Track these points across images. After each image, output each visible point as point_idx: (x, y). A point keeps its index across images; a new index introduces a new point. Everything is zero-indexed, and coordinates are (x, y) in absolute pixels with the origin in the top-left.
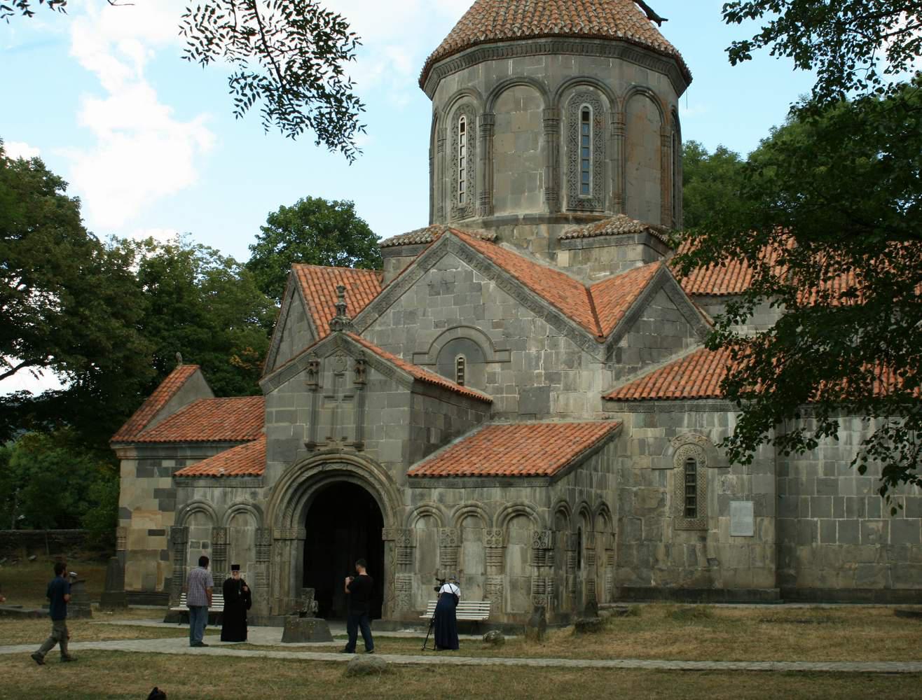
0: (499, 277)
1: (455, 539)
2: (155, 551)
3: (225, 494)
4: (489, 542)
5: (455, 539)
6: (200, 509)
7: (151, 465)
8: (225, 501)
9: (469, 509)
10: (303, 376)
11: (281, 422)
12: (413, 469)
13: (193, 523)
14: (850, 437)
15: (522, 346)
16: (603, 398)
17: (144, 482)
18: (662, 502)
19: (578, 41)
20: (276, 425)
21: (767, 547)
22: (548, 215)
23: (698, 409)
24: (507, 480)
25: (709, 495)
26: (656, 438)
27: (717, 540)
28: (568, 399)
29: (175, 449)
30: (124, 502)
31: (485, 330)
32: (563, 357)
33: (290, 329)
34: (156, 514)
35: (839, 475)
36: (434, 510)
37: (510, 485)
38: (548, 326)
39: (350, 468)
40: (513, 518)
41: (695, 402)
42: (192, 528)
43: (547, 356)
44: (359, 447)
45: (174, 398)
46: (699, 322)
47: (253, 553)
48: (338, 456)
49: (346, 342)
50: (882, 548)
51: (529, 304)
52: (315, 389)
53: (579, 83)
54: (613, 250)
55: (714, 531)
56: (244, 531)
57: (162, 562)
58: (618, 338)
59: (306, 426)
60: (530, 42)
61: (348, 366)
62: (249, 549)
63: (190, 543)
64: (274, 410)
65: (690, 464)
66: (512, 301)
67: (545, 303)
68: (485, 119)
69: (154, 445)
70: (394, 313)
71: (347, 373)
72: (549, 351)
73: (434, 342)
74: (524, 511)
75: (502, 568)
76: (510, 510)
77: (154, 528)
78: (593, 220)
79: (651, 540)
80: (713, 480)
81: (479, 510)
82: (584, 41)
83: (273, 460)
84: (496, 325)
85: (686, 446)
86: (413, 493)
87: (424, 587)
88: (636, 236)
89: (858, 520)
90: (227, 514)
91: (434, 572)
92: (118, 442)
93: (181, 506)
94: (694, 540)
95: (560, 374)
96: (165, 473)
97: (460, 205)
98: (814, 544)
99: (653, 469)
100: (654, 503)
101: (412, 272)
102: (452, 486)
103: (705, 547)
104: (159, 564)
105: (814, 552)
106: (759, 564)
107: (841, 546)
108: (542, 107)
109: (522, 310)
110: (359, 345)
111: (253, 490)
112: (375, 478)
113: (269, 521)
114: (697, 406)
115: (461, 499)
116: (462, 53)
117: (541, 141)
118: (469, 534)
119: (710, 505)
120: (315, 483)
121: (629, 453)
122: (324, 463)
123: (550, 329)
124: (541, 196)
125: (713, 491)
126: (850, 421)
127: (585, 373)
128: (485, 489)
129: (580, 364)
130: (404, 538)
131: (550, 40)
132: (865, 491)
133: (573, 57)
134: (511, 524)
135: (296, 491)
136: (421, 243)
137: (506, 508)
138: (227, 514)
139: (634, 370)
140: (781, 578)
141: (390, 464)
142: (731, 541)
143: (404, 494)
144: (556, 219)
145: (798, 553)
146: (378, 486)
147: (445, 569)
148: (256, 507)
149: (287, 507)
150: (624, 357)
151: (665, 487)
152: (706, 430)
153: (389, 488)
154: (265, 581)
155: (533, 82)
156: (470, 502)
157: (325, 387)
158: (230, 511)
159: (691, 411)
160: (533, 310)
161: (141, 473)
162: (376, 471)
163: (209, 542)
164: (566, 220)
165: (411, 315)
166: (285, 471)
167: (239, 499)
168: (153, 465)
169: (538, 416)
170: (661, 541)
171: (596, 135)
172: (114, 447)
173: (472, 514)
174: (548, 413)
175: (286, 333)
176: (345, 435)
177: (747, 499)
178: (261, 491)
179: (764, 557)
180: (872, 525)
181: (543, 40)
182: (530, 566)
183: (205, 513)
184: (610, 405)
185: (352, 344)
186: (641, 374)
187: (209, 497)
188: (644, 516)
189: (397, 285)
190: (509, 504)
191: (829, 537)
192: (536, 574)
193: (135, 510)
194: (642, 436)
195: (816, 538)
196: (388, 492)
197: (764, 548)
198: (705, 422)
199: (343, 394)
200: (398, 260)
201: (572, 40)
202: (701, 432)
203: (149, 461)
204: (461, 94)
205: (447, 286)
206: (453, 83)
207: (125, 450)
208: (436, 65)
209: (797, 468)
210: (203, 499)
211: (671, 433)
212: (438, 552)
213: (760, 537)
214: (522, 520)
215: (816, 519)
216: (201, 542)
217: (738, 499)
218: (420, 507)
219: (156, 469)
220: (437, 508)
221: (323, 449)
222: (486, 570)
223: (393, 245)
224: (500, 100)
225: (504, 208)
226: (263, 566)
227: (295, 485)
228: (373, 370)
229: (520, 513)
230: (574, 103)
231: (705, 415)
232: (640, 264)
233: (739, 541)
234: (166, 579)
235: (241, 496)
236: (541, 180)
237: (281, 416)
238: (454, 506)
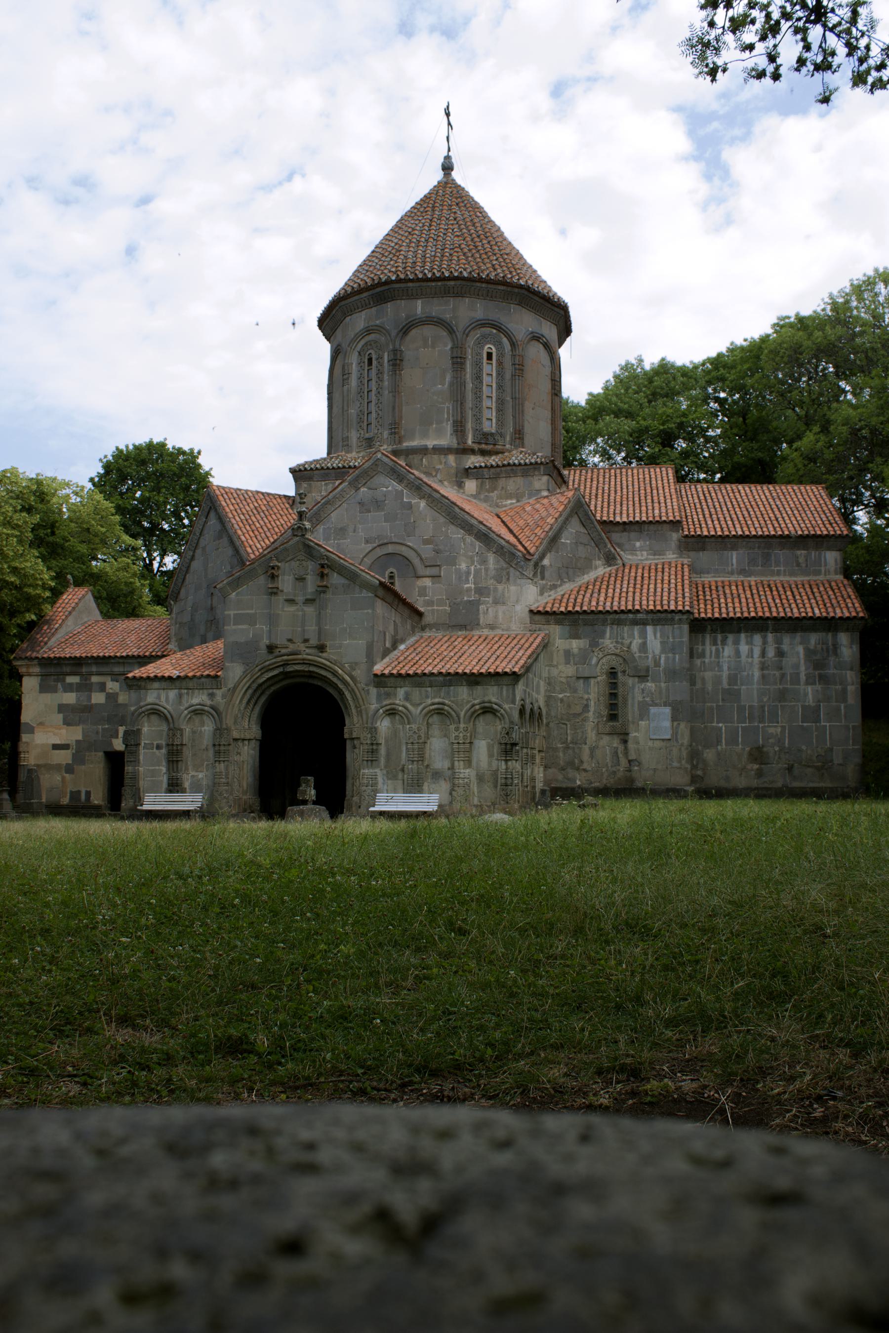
0: (430, 496)
1: (423, 736)
2: (60, 765)
3: (180, 696)
4: (457, 737)
5: (423, 736)
6: (155, 712)
8: (180, 703)
9: (436, 706)
10: (262, 580)
12: (378, 668)
13: (146, 724)
14: (751, 651)
15: (452, 562)
16: (531, 611)
17: (47, 698)
18: (586, 707)
19: (484, 285)
20: (234, 627)
21: (683, 749)
22: (455, 446)
23: (619, 623)
24: (474, 679)
25: (630, 702)
26: (580, 649)
27: (638, 743)
28: (497, 612)
30: (26, 716)
31: (415, 547)
32: (492, 573)
33: (204, 548)
34: (60, 729)
35: (742, 684)
36: (400, 708)
37: (477, 683)
38: (477, 543)
39: (312, 669)
40: (478, 715)
41: (617, 616)
42: (145, 730)
43: (477, 572)
44: (321, 648)
45: (69, 618)
46: (606, 546)
47: (211, 753)
49: (309, 546)
50: (780, 751)
51: (459, 522)
52: (274, 592)
53: (483, 325)
54: (520, 480)
55: (636, 734)
56: (201, 731)
57: (67, 775)
58: (542, 557)
60: (439, 284)
62: (207, 749)
63: (143, 744)
64: (232, 613)
65: (612, 673)
66: (442, 520)
67: (476, 523)
68: (395, 355)
69: (59, 662)
70: (324, 529)
71: (309, 577)
72: (479, 567)
73: (365, 557)
74: (492, 708)
75: (468, 763)
76: (477, 707)
77: (58, 742)
78: (497, 453)
79: (576, 743)
80: (633, 687)
81: (446, 708)
82: (490, 286)
83: (232, 662)
84: (426, 542)
85: (609, 657)
86: (378, 692)
87: (390, 782)
88: (542, 467)
89: (758, 726)
90: (183, 715)
91: (401, 767)
92: (21, 659)
93: (133, 709)
94: (616, 742)
95: (489, 589)
96: (69, 688)
97: (367, 436)
98: (719, 747)
99: (578, 678)
100: (578, 709)
101: (342, 490)
102: (419, 685)
103: (626, 748)
104: (63, 778)
105: (718, 754)
106: (675, 764)
107: (743, 749)
108: (449, 346)
109: (452, 527)
110: (322, 550)
111: (211, 691)
112: (339, 678)
113: (229, 721)
114: (619, 620)
115: (427, 697)
116: (371, 292)
117: (448, 378)
118: (435, 731)
119: (631, 710)
120: (272, 685)
121: (555, 663)
122: (286, 664)
123: (480, 547)
124: (449, 428)
125: (633, 698)
126: (752, 637)
127: (513, 588)
128: (452, 688)
129: (508, 579)
130: (369, 736)
131: (459, 282)
132: (765, 700)
133: (479, 301)
134: (477, 723)
135: (255, 691)
136: (333, 468)
137: (473, 705)
138: (183, 715)
139: (554, 587)
140: (694, 779)
141: (354, 665)
142: (650, 743)
143: (368, 693)
144: (465, 451)
145: (705, 755)
146: (341, 686)
147: (413, 764)
148: (212, 707)
149: (245, 708)
150: (547, 574)
151: (589, 693)
152: (627, 642)
153: (354, 687)
154: (223, 780)
155: (439, 322)
156: (437, 700)
158: (186, 712)
159: (613, 624)
160: (463, 528)
161: (44, 688)
162: (340, 671)
163: (164, 743)
164: (472, 452)
165: (341, 532)
166: (244, 672)
167: (195, 701)
168: (57, 681)
169: (468, 627)
170: (586, 744)
171: (498, 374)
172: (16, 663)
173: (440, 712)
174: (478, 624)
175: (199, 552)
176: (306, 637)
177: (665, 705)
178: (219, 693)
179: (680, 760)
180: (771, 730)
181: (452, 283)
182: (498, 760)
183: (159, 715)
184: (537, 618)
185: (314, 549)
186: (561, 591)
187: (163, 699)
188: (569, 721)
189: (327, 503)
190: (476, 702)
191: (732, 740)
192: (504, 767)
194: (567, 647)
195: (721, 741)
196: (352, 692)
197: (680, 749)
198: (626, 635)
200: (310, 485)
201: (478, 284)
202: (622, 644)
203: (53, 677)
204: (368, 331)
205: (378, 504)
206: (359, 321)
207: (28, 666)
208: (343, 303)
209: (703, 679)
210: (157, 702)
211: (594, 644)
212: (404, 748)
213: (677, 740)
214: (489, 717)
215: (720, 725)
216: (155, 743)
217: (656, 705)
218: (386, 705)
219: (60, 685)
220: (403, 706)
221: (283, 651)
222: (453, 765)
223: (306, 469)
224: (408, 338)
225: (412, 438)
226: (221, 767)
227: (255, 686)
228: (335, 574)
229: (488, 710)
230: (480, 343)
231: (626, 628)
232: (545, 493)
233: (658, 744)
234: (71, 792)
235: (199, 698)
236: (448, 413)
237: (239, 619)
238: (421, 704)
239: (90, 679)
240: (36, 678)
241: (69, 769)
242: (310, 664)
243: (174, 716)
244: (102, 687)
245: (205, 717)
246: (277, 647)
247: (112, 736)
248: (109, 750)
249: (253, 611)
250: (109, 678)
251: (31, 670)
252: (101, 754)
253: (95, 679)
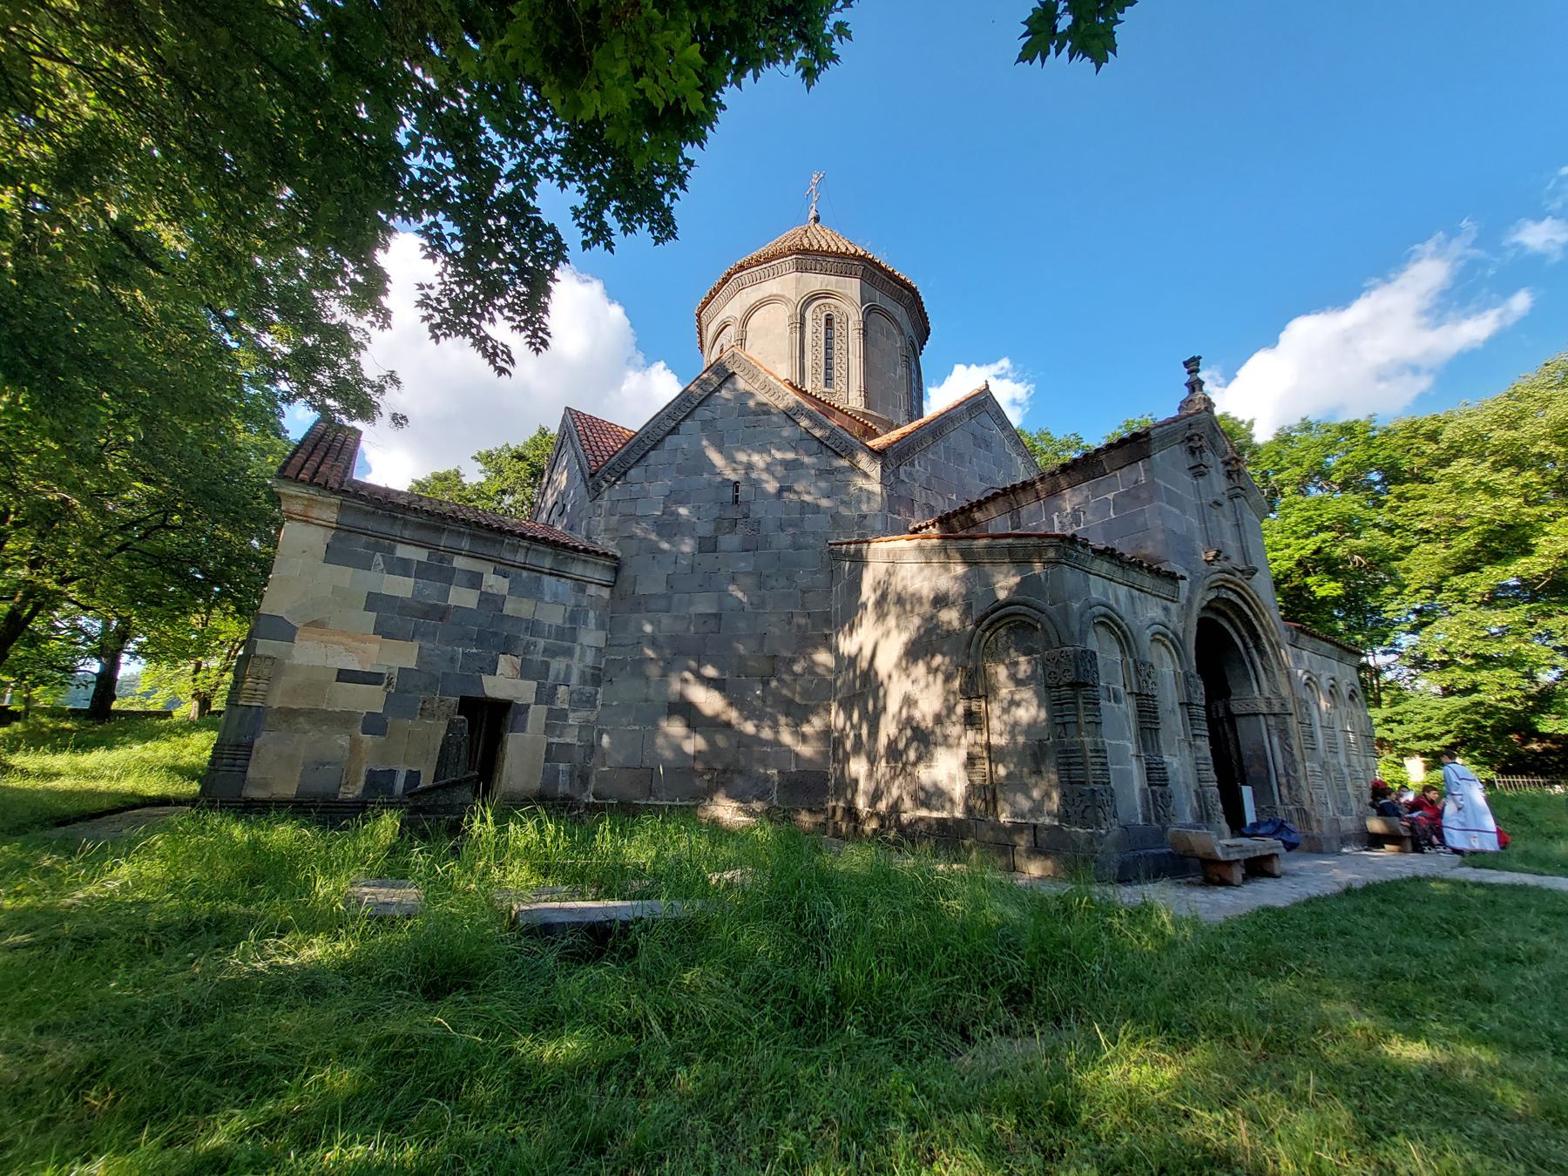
7: (367, 546)
10: (1179, 452)
17: (344, 576)
29: (439, 530)
59: (1196, 523)
77: (355, 666)
96: (403, 568)
104: (355, 743)
161: (333, 554)
168: (376, 548)
193: (307, 625)
207: (312, 502)
219: (378, 557)
234: (371, 774)
239: (450, 562)
240: (322, 530)
241: (374, 724)
243: (1135, 634)
244: (475, 580)
245: (1163, 649)
247: (482, 670)
248: (473, 694)
250: (490, 567)
251: (315, 513)
252: (455, 700)
253: (459, 562)
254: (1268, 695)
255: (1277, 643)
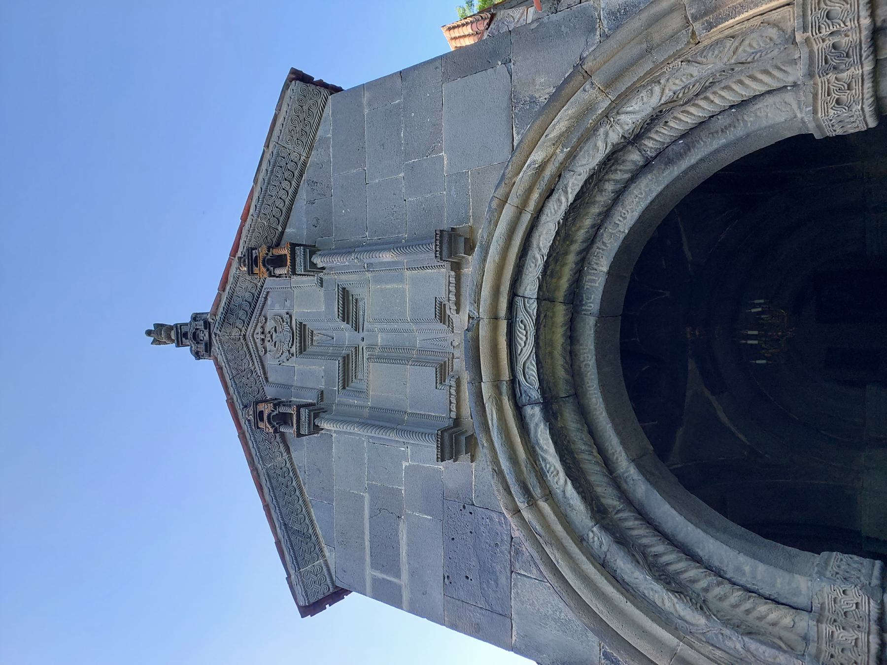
11: (396, 548)
39: (530, 287)
48: (484, 331)
61: (283, 312)
135: (622, 540)
149: (702, 605)
157: (322, 386)
176: (430, 311)
199: (344, 325)
242: (513, 294)
246: (457, 421)
249: (367, 496)
254: (797, 73)
255: (610, 84)
